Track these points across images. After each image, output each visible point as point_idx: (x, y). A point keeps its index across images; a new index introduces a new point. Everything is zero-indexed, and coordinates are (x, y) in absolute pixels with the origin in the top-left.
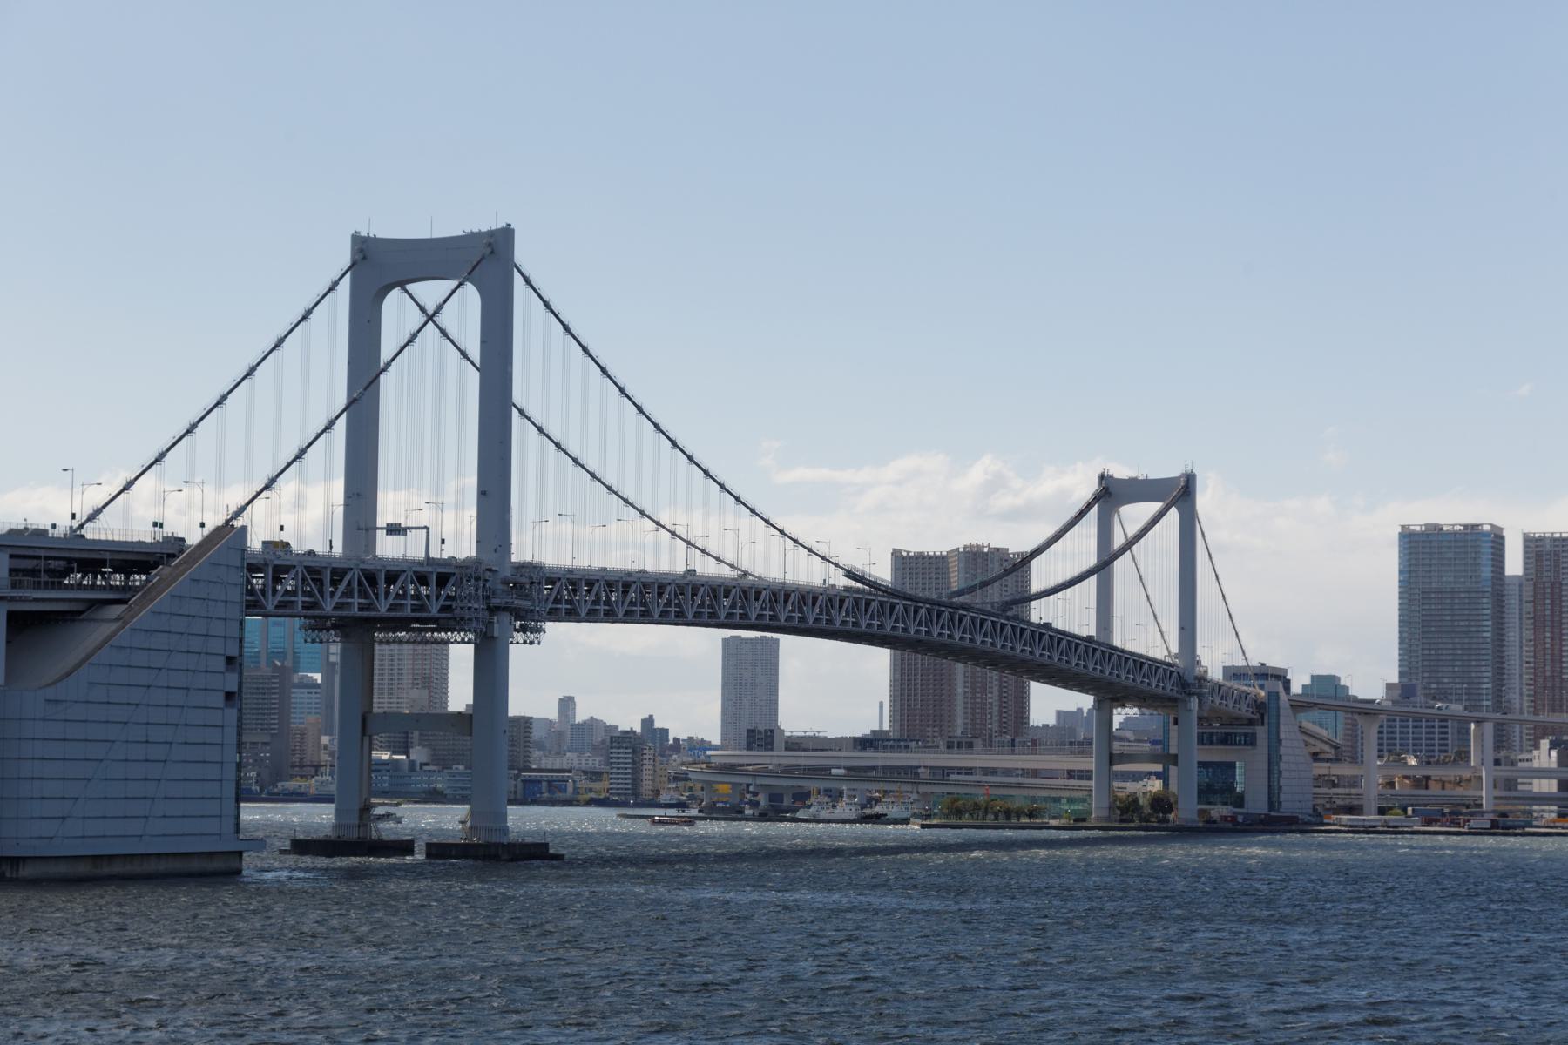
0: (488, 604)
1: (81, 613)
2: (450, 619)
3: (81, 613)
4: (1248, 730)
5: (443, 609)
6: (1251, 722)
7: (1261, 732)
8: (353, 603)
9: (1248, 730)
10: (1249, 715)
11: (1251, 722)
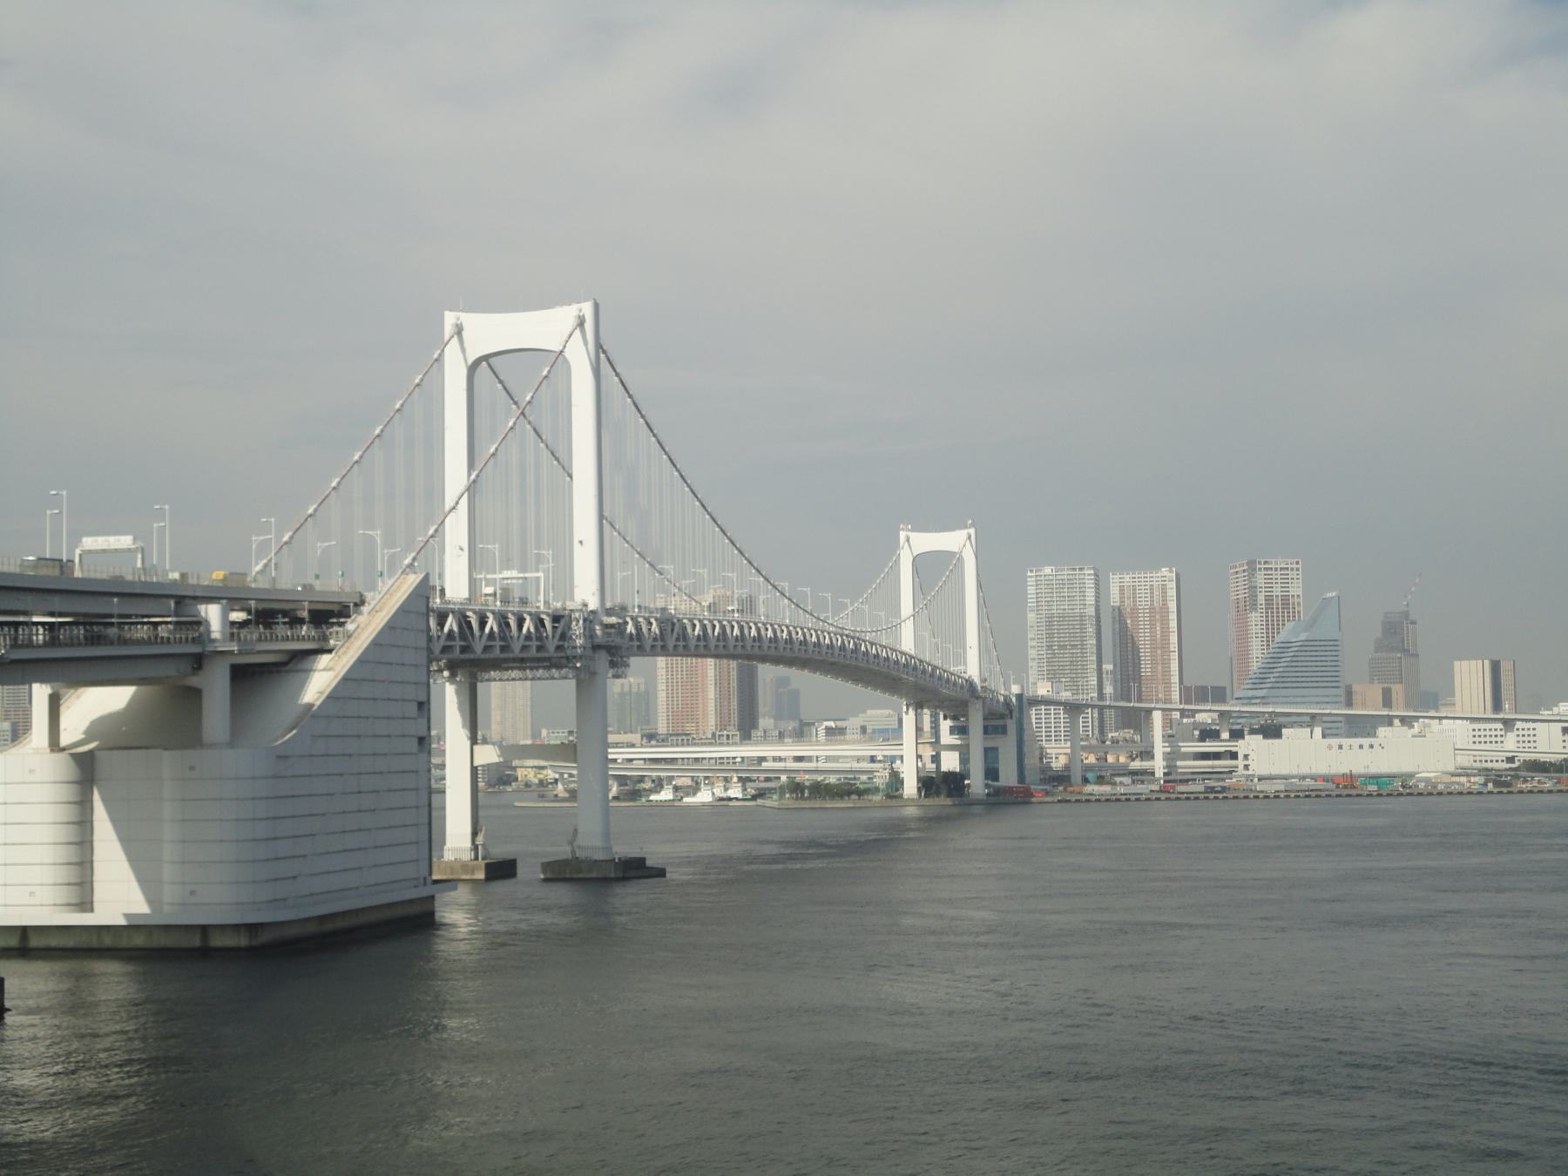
0: (592, 643)
1: (285, 664)
2: (562, 657)
3: (285, 664)
4: (1001, 722)
5: (559, 648)
6: (1002, 716)
7: (1011, 726)
8: (456, 646)
9: (1001, 722)
10: (1003, 711)
11: (1002, 716)
